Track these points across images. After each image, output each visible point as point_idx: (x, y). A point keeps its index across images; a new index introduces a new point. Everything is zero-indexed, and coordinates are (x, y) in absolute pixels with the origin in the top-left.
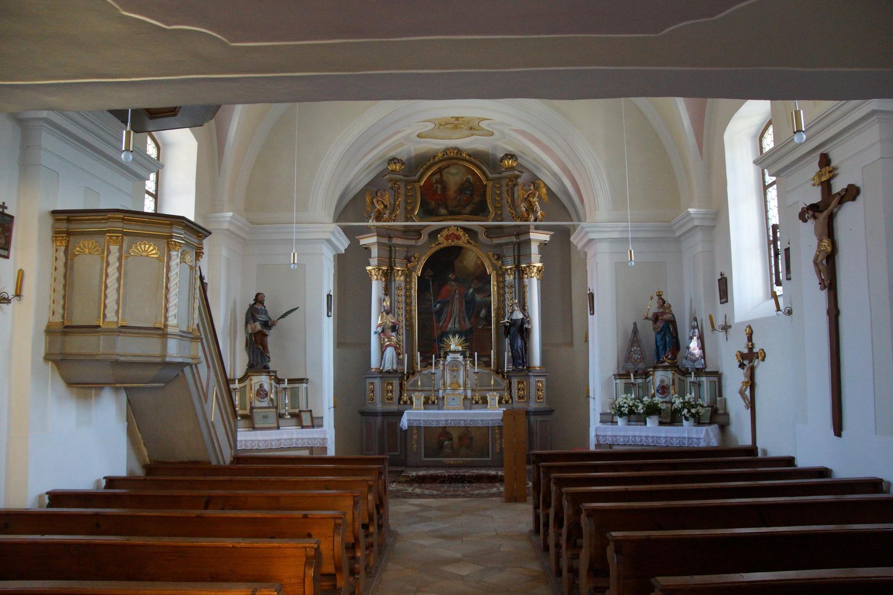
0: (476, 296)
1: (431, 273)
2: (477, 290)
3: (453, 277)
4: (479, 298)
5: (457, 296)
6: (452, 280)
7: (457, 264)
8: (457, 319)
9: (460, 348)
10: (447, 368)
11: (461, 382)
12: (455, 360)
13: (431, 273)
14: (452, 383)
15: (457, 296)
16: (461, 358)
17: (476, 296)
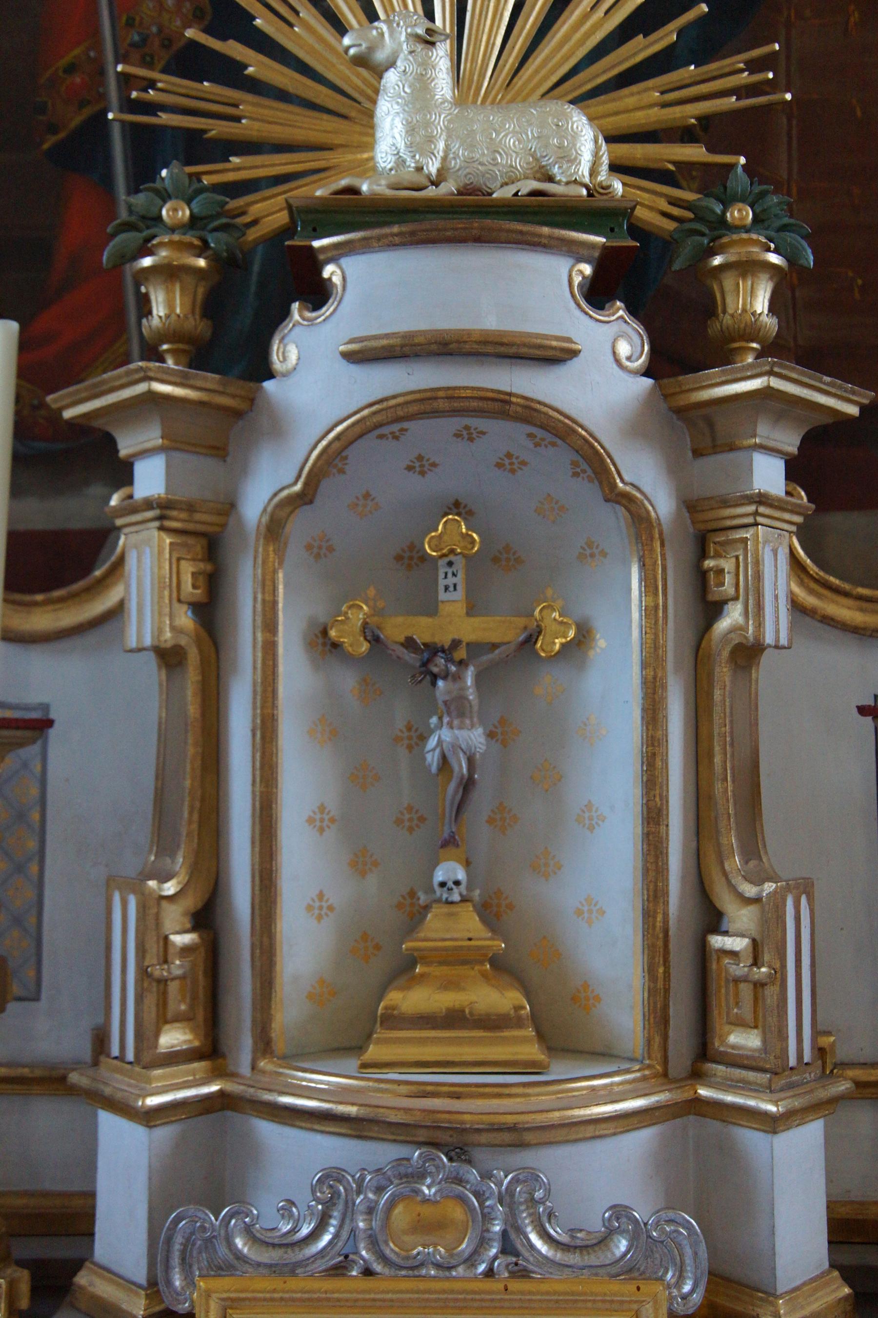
9: (581, 150)
10: (281, 610)
11: (599, 903)
12: (463, 397)
14: (389, 950)
16: (604, 368)
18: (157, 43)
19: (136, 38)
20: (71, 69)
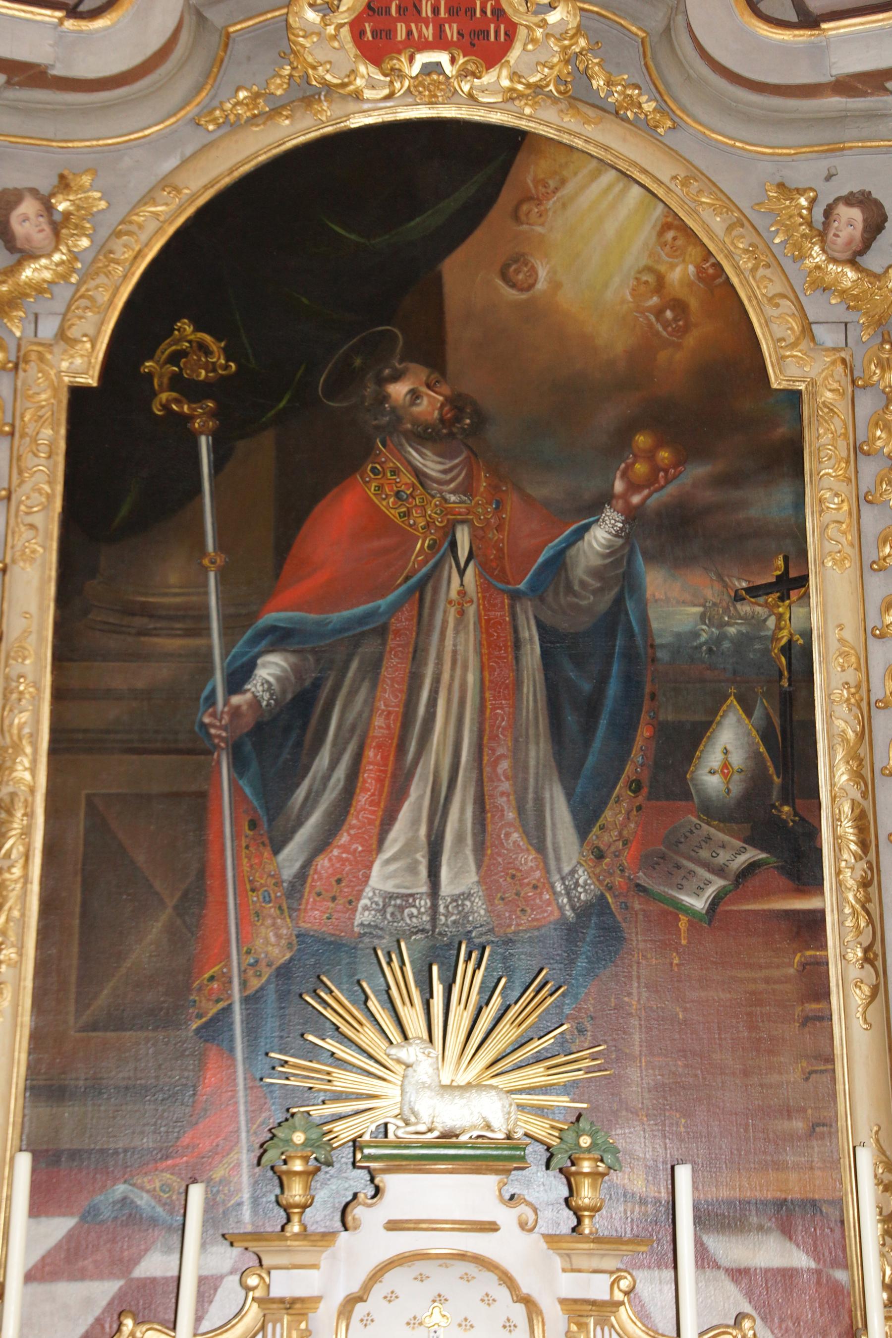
0: (656, 582)
1: (214, 360)
2: (674, 533)
3: (429, 406)
4: (677, 605)
5: (461, 583)
6: (425, 435)
7: (466, 278)
8: (460, 815)
13: (214, 360)
15: (461, 583)
17: (656, 582)
18: (264, 963)
19: (252, 961)
20: (212, 978)
